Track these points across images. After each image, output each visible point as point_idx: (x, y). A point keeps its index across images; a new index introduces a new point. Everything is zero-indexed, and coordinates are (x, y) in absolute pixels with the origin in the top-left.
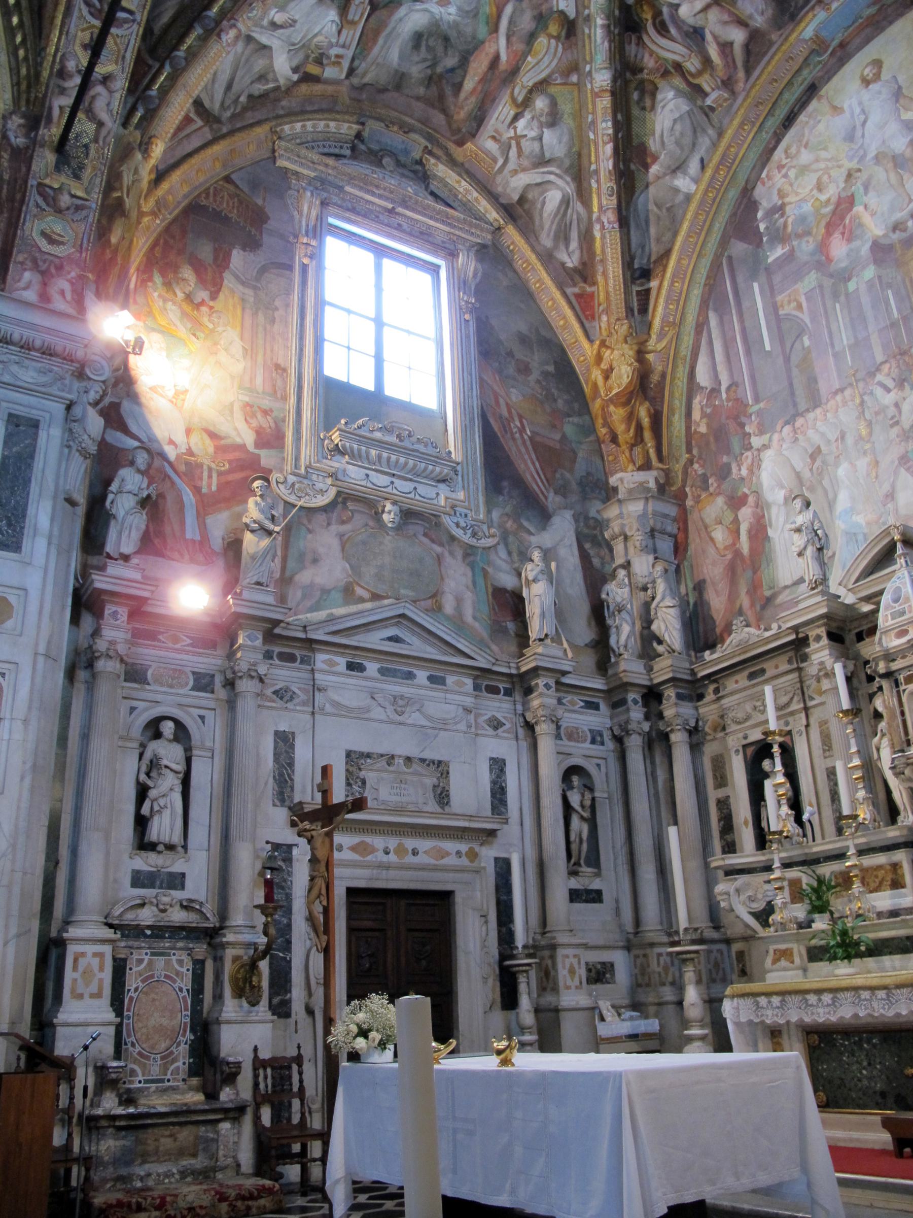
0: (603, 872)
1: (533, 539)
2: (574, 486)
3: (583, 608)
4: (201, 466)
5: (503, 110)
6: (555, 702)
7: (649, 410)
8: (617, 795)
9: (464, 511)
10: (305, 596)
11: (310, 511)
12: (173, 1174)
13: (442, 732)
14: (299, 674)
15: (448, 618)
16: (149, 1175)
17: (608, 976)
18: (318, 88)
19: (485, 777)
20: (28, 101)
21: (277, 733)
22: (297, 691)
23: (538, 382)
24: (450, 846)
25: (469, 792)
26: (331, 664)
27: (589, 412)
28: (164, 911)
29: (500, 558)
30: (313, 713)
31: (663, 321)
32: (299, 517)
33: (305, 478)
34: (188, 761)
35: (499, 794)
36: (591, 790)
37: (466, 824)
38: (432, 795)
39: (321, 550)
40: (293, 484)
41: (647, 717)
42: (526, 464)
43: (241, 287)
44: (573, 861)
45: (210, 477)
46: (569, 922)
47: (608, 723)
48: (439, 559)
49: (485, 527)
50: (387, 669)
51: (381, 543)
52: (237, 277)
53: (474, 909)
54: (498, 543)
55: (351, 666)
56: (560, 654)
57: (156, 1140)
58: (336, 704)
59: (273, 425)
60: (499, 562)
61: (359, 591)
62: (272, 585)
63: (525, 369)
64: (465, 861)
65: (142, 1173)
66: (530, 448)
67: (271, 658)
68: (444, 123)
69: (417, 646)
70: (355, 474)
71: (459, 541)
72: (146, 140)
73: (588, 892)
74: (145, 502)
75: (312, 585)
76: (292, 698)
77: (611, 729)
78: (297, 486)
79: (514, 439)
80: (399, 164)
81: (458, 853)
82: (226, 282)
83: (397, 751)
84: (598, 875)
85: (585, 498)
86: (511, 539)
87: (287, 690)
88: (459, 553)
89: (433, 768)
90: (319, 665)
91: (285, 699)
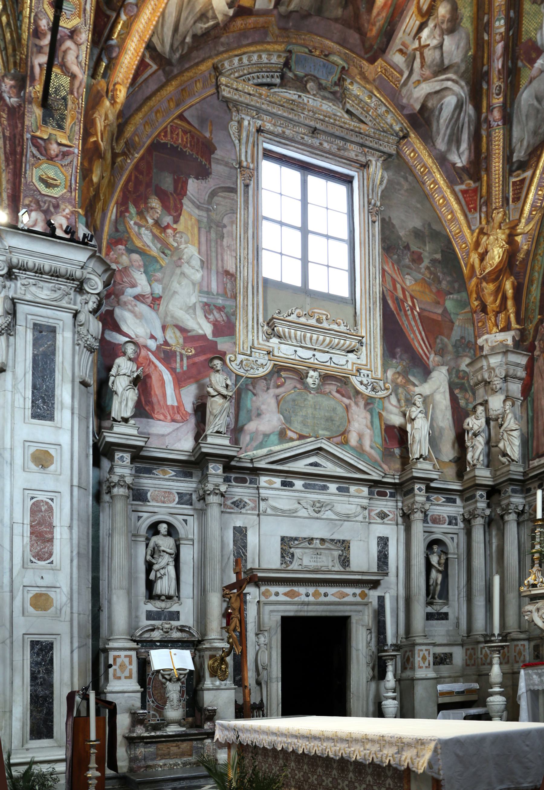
0: (450, 602)
1: (417, 390)
2: (450, 348)
3: (449, 435)
5: (410, 21)
6: (424, 499)
8: (463, 557)
9: (366, 372)
10: (252, 439)
11: (255, 380)
13: (346, 523)
15: (353, 448)
17: (448, 660)
18: (251, 20)
20: (15, 63)
21: (235, 528)
23: (428, 268)
24: (349, 591)
25: (363, 559)
26: (271, 483)
27: (466, 289)
28: (167, 632)
29: (392, 405)
30: (259, 515)
31: (532, 206)
32: (247, 385)
34: (178, 547)
36: (446, 553)
39: (263, 407)
40: (242, 361)
41: (489, 506)
43: (196, 211)
44: (430, 596)
45: (182, 360)
46: (424, 631)
47: (461, 511)
48: (347, 408)
49: (381, 383)
50: (309, 484)
51: (305, 400)
52: (193, 202)
53: (363, 626)
54: (391, 394)
55: (284, 484)
56: (431, 467)
58: (274, 508)
59: (225, 318)
60: (390, 407)
61: (290, 434)
62: (229, 433)
63: (417, 259)
64: (358, 599)
66: (419, 321)
67: (230, 481)
68: (358, 42)
69: (330, 468)
70: (285, 351)
72: (111, 87)
73: (439, 614)
75: (257, 432)
76: (244, 506)
77: (463, 515)
78: (244, 363)
79: (406, 315)
80: (321, 87)
82: (184, 207)
83: (315, 536)
84: (446, 604)
85: (458, 356)
86: (400, 390)
87: (241, 501)
88: (362, 403)
91: (240, 507)
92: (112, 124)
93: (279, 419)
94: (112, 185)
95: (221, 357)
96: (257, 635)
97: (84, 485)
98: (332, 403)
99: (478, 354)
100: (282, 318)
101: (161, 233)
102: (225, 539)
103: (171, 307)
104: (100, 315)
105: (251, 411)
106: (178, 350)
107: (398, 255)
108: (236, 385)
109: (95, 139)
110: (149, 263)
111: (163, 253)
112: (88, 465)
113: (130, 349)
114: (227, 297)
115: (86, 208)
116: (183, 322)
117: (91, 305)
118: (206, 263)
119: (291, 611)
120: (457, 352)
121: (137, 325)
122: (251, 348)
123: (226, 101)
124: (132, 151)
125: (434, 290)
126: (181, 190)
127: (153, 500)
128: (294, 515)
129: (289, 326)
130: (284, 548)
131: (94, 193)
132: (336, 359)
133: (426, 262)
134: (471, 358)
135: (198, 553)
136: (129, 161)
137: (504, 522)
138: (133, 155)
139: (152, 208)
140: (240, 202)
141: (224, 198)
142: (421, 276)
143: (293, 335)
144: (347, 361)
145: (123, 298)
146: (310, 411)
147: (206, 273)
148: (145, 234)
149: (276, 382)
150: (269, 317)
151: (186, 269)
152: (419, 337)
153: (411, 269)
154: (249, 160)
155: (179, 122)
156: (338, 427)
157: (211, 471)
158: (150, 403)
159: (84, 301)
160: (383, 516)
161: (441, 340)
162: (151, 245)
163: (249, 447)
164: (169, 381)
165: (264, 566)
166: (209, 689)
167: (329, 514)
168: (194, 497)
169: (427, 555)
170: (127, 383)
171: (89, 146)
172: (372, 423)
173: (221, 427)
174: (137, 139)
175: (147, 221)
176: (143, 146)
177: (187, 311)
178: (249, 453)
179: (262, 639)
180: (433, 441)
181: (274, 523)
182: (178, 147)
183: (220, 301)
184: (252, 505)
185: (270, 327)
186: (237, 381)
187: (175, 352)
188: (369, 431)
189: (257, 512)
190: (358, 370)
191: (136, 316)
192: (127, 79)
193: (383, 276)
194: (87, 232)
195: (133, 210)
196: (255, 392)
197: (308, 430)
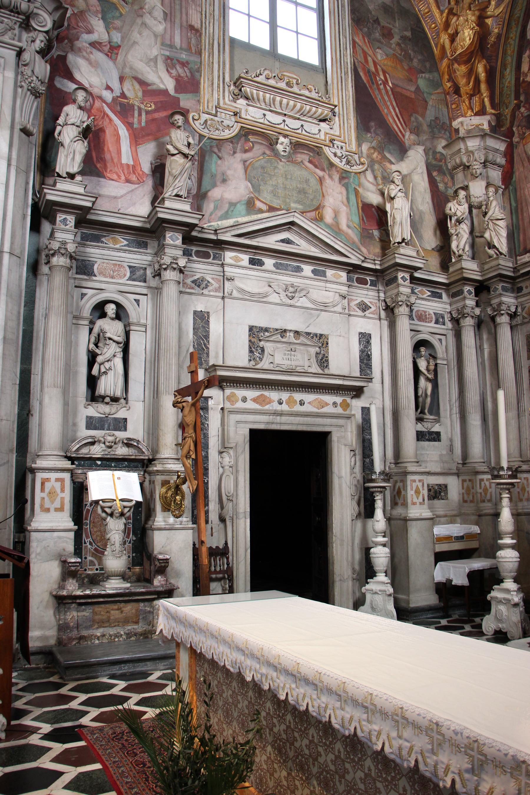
1: (394, 168)
2: (425, 128)
7: (485, 67)
10: (216, 208)
11: (220, 142)
12: (122, 635)
14: (212, 268)
15: (328, 226)
16: (103, 636)
19: (356, 348)
21: (195, 312)
22: (210, 280)
26: (237, 259)
27: (438, 70)
30: (223, 298)
34: (127, 334)
35: (366, 359)
37: (340, 382)
38: (315, 361)
39: (229, 173)
42: (388, 108)
48: (321, 180)
49: (356, 157)
51: (275, 168)
54: (367, 170)
55: (252, 262)
57: (107, 612)
61: (258, 204)
65: (99, 634)
66: (392, 97)
67: (191, 255)
70: (253, 114)
71: (336, 167)
75: (222, 199)
76: (207, 286)
78: (209, 122)
81: (335, 404)
86: (376, 167)
87: (203, 279)
88: (336, 177)
89: (316, 339)
90: (228, 260)
91: (202, 286)
93: (247, 187)
95: (184, 113)
96: (221, 453)
97: (17, 252)
98: (304, 173)
99: (454, 137)
100: (250, 78)
102: (183, 326)
105: (216, 175)
107: (368, 29)
112: (23, 227)
114: (192, 53)
118: (169, 15)
119: (261, 422)
120: (432, 132)
122: (216, 108)
125: (406, 68)
127: (101, 273)
128: (264, 300)
129: (257, 87)
130: (253, 340)
132: (307, 126)
133: (396, 39)
134: (447, 141)
135: (152, 342)
137: (496, 325)
142: (392, 52)
143: (261, 98)
144: (320, 130)
146: (281, 180)
147: (169, 26)
149: (243, 146)
150: (236, 77)
151: (148, 19)
152: (393, 113)
153: (382, 43)
156: (312, 200)
157: (168, 240)
158: (102, 160)
160: (364, 307)
161: (416, 118)
165: (229, 363)
166: (160, 529)
167: (304, 302)
168: (149, 272)
169: (414, 358)
172: (348, 199)
178: (212, 224)
179: (227, 460)
180: (415, 225)
181: (242, 308)
183: (184, 56)
184: (215, 285)
185: (237, 87)
187: (133, 106)
188: (345, 208)
189: (221, 295)
190: (332, 141)
191: (90, 63)
193: (354, 47)
197: (278, 201)
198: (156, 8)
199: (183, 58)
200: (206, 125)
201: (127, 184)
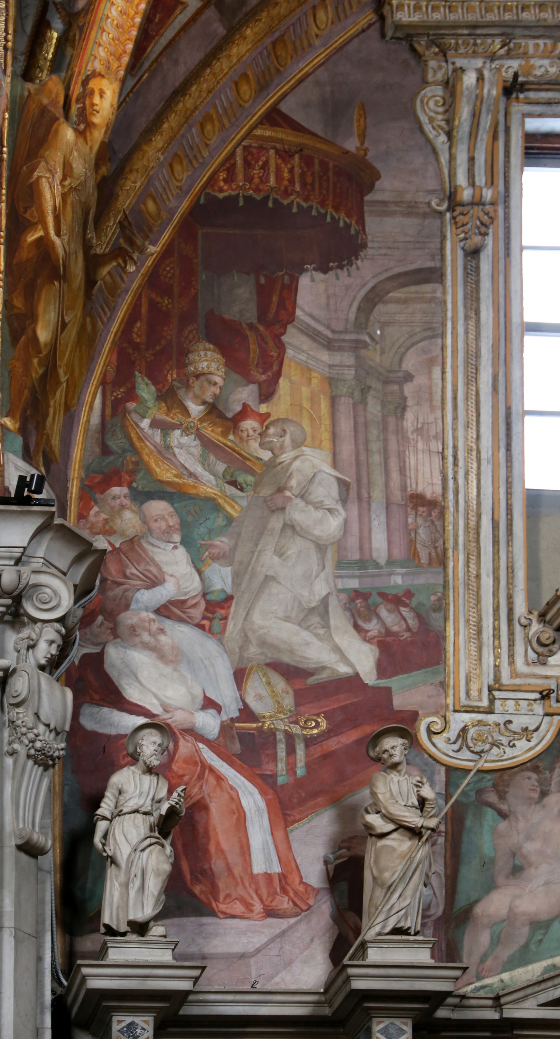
4: (272, 733)
10: (496, 941)
11: (502, 777)
32: (479, 792)
33: (490, 711)
39: (530, 847)
40: (464, 730)
43: (325, 356)
45: (291, 751)
52: (313, 335)
62: (429, 931)
72: (77, 90)
74: (167, 825)
75: (511, 917)
78: (472, 732)
82: (290, 352)
92: (83, 184)
94: (88, 341)
95: (405, 726)
101: (225, 434)
103: (257, 618)
104: (67, 671)
105: (493, 861)
106: (281, 726)
108: (448, 796)
109: (40, 233)
110: (195, 516)
111: (234, 483)
113: (150, 745)
114: (419, 565)
115: (24, 410)
116: (292, 652)
117: (44, 651)
118: (354, 487)
121: (169, 680)
123: (408, 36)
124: (139, 242)
126: (277, 309)
131: (41, 372)
136: (131, 268)
138: (142, 250)
139: (198, 376)
140: (454, 303)
141: (405, 302)
145: (128, 618)
147: (355, 512)
148: (181, 446)
151: (300, 514)
154: (481, 179)
155: (268, 133)
159: (25, 644)
162: (199, 470)
163: (489, 962)
164: (258, 809)
170: (143, 830)
171: (24, 254)
173: (406, 916)
174: (151, 206)
175: (186, 411)
176: (170, 220)
177: (303, 623)
182: (266, 198)
183: (398, 580)
186: (450, 785)
192: (119, 59)
194: (28, 470)
195: (146, 390)
196: (504, 807)
198: (319, 477)
199: (397, 586)
200: (465, 739)
201: (270, 920)
